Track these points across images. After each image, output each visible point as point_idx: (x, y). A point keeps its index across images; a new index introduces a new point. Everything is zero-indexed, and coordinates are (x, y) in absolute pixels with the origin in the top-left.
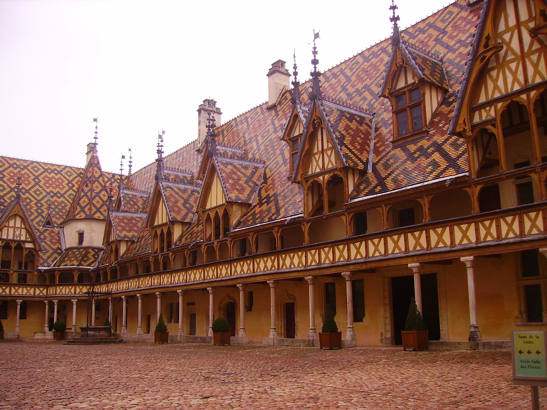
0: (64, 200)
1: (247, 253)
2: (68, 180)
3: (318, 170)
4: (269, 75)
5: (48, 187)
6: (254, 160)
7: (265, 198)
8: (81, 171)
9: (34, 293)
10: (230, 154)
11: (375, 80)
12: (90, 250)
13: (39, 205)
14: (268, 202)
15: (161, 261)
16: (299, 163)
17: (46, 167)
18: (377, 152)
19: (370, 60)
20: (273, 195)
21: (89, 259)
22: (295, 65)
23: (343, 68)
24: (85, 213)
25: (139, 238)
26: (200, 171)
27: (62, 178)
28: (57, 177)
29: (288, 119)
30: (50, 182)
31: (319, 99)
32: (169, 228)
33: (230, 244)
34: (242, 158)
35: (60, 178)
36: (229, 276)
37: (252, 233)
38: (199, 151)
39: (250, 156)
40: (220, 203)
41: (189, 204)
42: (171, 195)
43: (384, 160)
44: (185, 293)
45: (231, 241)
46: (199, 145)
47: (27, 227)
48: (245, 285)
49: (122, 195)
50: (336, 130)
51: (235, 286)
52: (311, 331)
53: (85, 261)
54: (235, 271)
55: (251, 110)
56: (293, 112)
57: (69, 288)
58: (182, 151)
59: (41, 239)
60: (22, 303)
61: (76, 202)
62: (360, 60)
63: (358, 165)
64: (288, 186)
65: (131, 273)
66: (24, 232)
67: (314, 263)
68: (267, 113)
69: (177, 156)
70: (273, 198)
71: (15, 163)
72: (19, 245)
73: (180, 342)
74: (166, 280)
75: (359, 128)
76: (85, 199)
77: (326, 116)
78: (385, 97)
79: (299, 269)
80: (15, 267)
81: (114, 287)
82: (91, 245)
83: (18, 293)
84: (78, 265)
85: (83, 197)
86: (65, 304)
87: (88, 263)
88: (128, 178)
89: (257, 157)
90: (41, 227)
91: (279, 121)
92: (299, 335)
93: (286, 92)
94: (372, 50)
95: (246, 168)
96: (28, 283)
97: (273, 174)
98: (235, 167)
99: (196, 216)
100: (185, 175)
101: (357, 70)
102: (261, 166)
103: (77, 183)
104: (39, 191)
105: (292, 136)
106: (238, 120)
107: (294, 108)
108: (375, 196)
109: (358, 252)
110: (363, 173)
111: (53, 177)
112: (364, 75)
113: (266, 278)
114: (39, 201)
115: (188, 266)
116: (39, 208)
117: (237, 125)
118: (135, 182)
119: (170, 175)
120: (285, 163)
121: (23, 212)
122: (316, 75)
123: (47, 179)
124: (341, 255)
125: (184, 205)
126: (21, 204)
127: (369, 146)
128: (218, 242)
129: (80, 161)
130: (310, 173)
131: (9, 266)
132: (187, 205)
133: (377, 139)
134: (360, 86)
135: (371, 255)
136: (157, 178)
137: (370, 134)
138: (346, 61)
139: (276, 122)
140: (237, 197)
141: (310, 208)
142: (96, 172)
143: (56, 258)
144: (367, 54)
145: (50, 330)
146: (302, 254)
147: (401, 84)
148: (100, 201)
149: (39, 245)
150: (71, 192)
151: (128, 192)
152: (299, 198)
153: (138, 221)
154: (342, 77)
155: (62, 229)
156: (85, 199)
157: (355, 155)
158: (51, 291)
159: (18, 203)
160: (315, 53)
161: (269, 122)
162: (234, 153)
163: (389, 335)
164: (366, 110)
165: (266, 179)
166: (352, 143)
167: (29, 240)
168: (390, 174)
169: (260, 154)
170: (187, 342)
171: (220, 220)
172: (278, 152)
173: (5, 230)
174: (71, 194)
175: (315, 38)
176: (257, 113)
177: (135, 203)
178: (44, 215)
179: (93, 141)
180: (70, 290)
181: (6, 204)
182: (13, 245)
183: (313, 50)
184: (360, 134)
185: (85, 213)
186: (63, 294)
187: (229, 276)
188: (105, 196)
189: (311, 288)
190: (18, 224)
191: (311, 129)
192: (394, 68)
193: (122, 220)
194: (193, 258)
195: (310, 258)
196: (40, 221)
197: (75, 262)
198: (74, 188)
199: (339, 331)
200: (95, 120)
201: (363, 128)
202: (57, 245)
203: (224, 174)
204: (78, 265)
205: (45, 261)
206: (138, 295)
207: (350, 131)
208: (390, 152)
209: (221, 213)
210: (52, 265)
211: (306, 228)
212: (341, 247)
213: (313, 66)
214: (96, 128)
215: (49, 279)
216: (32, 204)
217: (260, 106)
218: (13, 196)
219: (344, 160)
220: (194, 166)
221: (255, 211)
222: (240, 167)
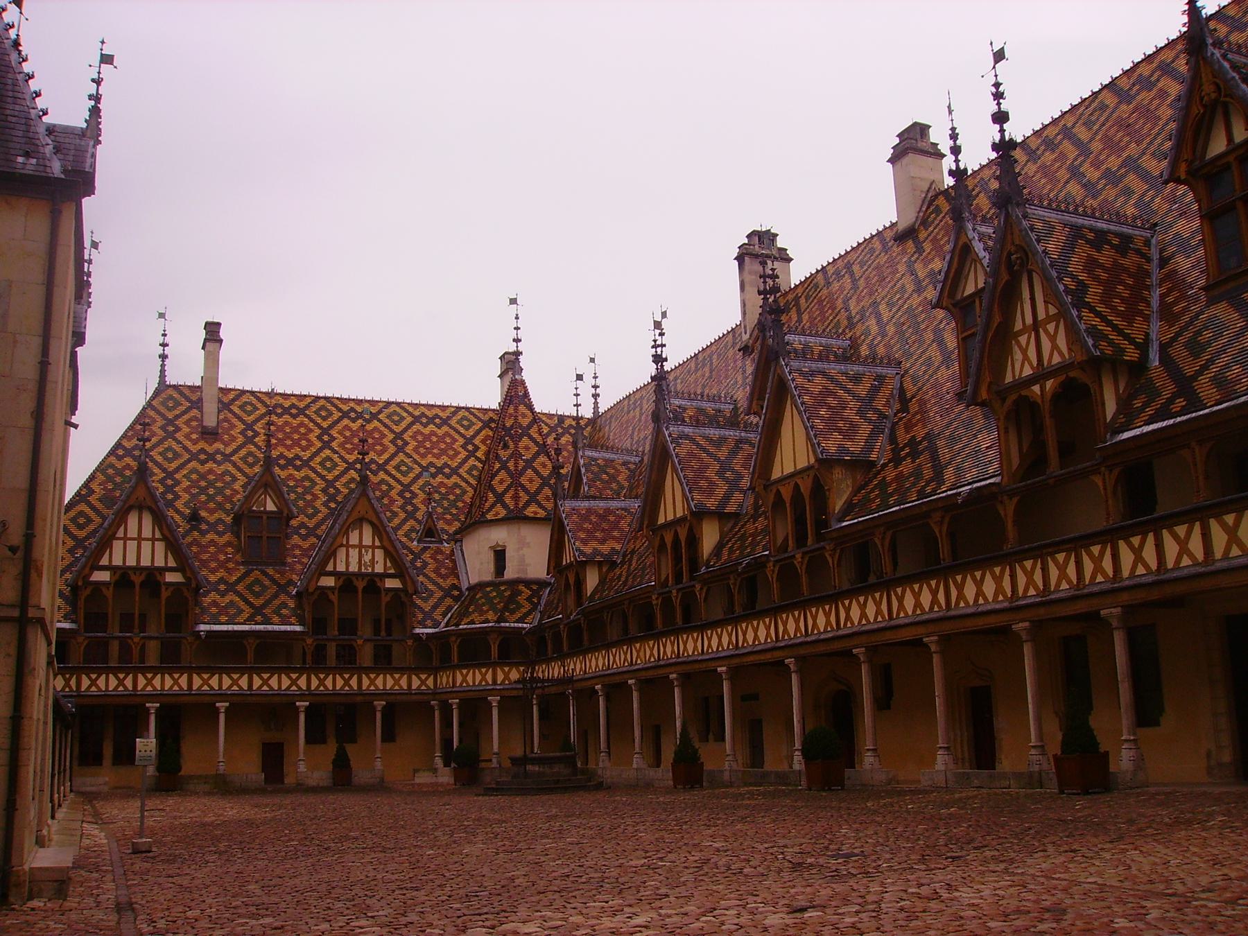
0: (459, 481)
1: (872, 575)
2: (463, 436)
3: (1027, 371)
4: (893, 160)
5: (423, 456)
6: (873, 359)
7: (905, 446)
8: (491, 414)
9: (410, 685)
10: (817, 350)
11: (1151, 143)
12: (521, 587)
13: (408, 495)
14: (914, 455)
15: (677, 602)
16: (982, 358)
17: (417, 413)
18: (1167, 314)
19: (1134, 97)
20: (924, 439)
21: (519, 606)
22: (953, 129)
23: (1069, 125)
24: (505, 506)
25: (624, 556)
26: (752, 393)
27: (452, 432)
28: (440, 432)
29: (948, 258)
30: (428, 445)
31: (1018, 205)
32: (691, 530)
33: (832, 556)
34: (844, 358)
36: (833, 629)
37: (882, 529)
38: (746, 350)
39: (864, 351)
40: (802, 464)
41: (733, 470)
42: (691, 454)
43: (1188, 335)
44: (735, 673)
45: (835, 549)
46: (746, 337)
47: (386, 543)
48: (872, 650)
49: (582, 462)
50: (1063, 272)
51: (847, 653)
52: (1033, 752)
53: (512, 612)
54: (848, 618)
55: (859, 244)
56: (957, 240)
57: (480, 672)
58: (708, 352)
59: (416, 568)
60: (384, 707)
61: (484, 482)
62: (1110, 100)
63: (1123, 350)
64: (961, 413)
65: (613, 633)
66: (379, 554)
67: (1032, 592)
68: (897, 249)
69: (697, 365)
70: (925, 444)
71: (352, 409)
72: (373, 582)
73: (731, 785)
74: (690, 646)
75: (1119, 263)
76: (503, 474)
77: (1039, 241)
78: (1178, 181)
79: (997, 606)
80: (366, 630)
81: (575, 667)
82: (522, 576)
83: (376, 686)
84: (498, 621)
86: (474, 706)
88: (592, 422)
89: (881, 351)
91: (925, 265)
92: (1005, 764)
93: (936, 196)
94: (1136, 74)
95: (857, 379)
96: (395, 664)
97: (920, 389)
98: (831, 379)
99: (751, 500)
100: (717, 406)
101: (1103, 125)
102: (891, 372)
103: (483, 442)
104: (405, 464)
105: (959, 297)
106: (831, 270)
107: (960, 230)
108: (1171, 422)
109: (1139, 559)
110: (1138, 369)
111: (433, 433)
112: (1120, 134)
113: (921, 630)
114: (407, 487)
115: (738, 610)
116: (408, 502)
117: (828, 284)
118: (610, 432)
119: (685, 409)
120: (946, 360)
122: (1004, 147)
123: (420, 438)
124: (1098, 569)
125: (720, 473)
126: (371, 495)
127: (1148, 304)
128: (804, 554)
129: (487, 394)
130: (1009, 379)
131: (354, 631)
132: (728, 474)
133: (1169, 285)
134: (1113, 162)
135: (1170, 565)
136: (656, 417)
137: (1148, 274)
138: (1074, 107)
139: (918, 266)
140: (842, 449)
141: (1016, 462)
142: (524, 416)
143: (449, 608)
144: (1125, 84)
145: (446, 764)
146: (1002, 572)
147: (1218, 146)
148: (535, 477)
149: (414, 583)
150: (472, 461)
151: (595, 454)
152: (987, 439)
153: (621, 518)
154: (1067, 146)
156: (503, 474)
157: (1115, 328)
158: (444, 679)
159: (364, 494)
160: (998, 96)
161: (902, 268)
162: (828, 348)
163: (1226, 757)
164: (1135, 218)
165: (904, 401)
166: (1106, 299)
167: (392, 571)
168: (1205, 368)
169: (888, 346)
170: (745, 785)
171: (805, 501)
172: (929, 336)
173: (341, 553)
174: (474, 467)
175: (996, 62)
176: (872, 250)
177: (613, 478)
178: (419, 515)
179: (512, 347)
180: (484, 676)
181: (339, 498)
182: (360, 585)
183: (994, 90)
184: (1124, 276)
185: (505, 506)
186: (468, 685)
187: (833, 629)
188: (544, 466)
189: (1027, 650)
190: (367, 540)
191: (1005, 277)
192: (1196, 110)
193: (585, 517)
194: (748, 593)
195: (1022, 580)
196: (412, 530)
198: (479, 454)
199: (1102, 750)
200: (513, 301)
201: (1129, 261)
202: (449, 582)
203: (806, 398)
204: (498, 621)
205: (428, 615)
206: (630, 682)
207: (1099, 272)
208: (1202, 312)
209: (805, 486)
210: (443, 624)
211: (1008, 509)
212: (1096, 550)
213: (997, 127)
214: (517, 318)
215: (436, 654)
216: (393, 493)
217: (879, 233)
218: (352, 480)
219: (1090, 342)
220: (737, 384)
221: (884, 478)
222: (842, 378)
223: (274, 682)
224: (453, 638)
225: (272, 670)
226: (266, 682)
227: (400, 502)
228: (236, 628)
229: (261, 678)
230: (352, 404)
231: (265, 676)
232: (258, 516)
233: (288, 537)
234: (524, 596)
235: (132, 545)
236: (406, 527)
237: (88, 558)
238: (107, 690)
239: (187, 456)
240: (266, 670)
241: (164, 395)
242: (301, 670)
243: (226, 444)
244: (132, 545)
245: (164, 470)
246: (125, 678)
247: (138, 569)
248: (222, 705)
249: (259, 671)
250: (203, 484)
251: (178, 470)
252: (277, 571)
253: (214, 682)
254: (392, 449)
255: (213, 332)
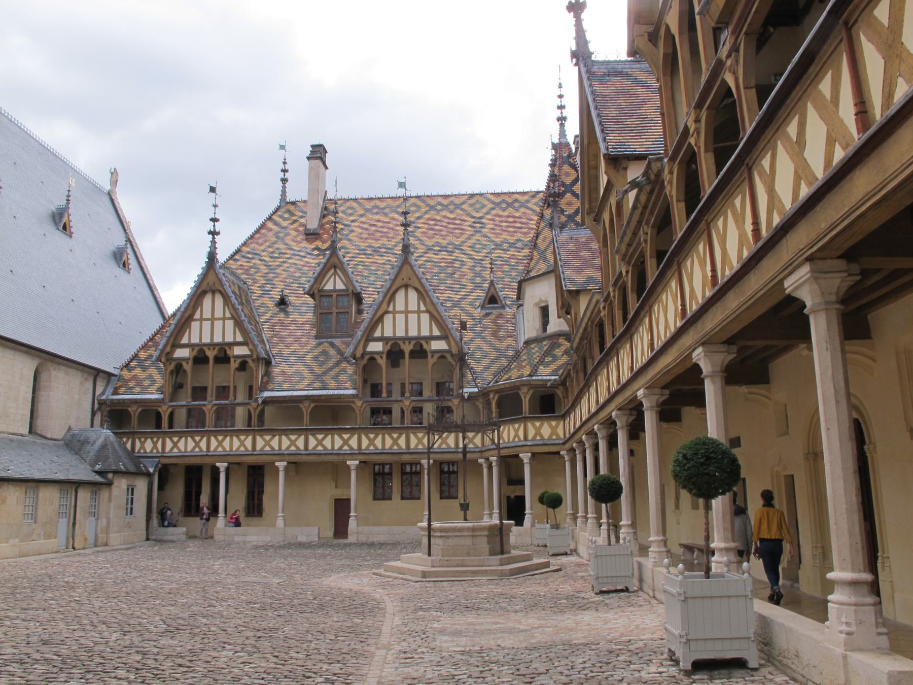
17: (498, 200)
35: (524, 215)
47: (431, 308)
53: (547, 365)
57: (514, 428)
66: (425, 317)
85: (543, 230)
87: (553, 367)
90: (479, 310)
111: (510, 215)
121: (419, 279)
126: (413, 262)
142: (567, 174)
155: (521, 308)
173: (388, 319)
182: (407, 348)
190: (413, 306)
197: (527, 371)
204: (530, 375)
214: (560, 86)
216: (465, 269)
223: (327, 443)
224: (491, 396)
225: (327, 431)
226: (320, 443)
227: (470, 275)
228: (295, 393)
229: (316, 439)
230: (439, 199)
231: (320, 437)
232: (328, 295)
233: (360, 312)
234: (563, 348)
235: (207, 325)
236: (473, 296)
237: (169, 338)
238: (186, 451)
239: (290, 253)
240: (320, 431)
241: (282, 210)
242: (352, 431)
243: (323, 242)
244: (207, 325)
245: (268, 266)
246: (200, 440)
247: (212, 345)
248: (281, 465)
249: (314, 432)
250: (298, 274)
251: (279, 266)
252: (344, 343)
253: (275, 443)
254: (470, 231)
255: (318, 153)
